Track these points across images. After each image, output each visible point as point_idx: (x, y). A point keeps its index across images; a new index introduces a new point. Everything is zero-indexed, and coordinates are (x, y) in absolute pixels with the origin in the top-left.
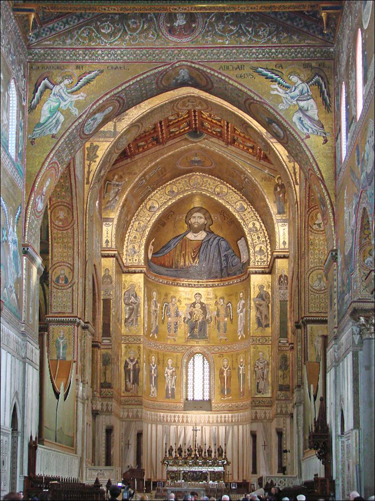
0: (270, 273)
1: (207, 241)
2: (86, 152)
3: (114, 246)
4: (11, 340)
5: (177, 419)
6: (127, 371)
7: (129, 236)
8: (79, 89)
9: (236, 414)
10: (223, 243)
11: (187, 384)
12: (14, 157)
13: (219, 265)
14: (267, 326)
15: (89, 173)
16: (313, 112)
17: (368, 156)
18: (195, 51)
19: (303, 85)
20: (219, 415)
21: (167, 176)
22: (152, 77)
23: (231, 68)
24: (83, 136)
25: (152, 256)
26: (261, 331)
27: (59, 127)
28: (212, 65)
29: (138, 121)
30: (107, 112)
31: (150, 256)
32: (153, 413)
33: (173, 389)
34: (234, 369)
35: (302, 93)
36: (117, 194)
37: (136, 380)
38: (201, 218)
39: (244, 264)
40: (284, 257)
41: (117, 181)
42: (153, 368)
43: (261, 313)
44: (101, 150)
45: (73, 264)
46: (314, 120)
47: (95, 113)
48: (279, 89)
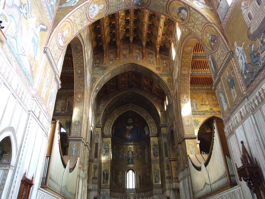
0: (157, 137)
1: (132, 129)
3: (101, 124)
5: (123, 196)
6: (104, 175)
7: (106, 124)
9: (147, 193)
11: (126, 182)
14: (157, 156)
15: (92, 86)
25: (114, 133)
26: (155, 158)
27: (76, 3)
31: (113, 133)
33: (121, 184)
36: (102, 106)
37: (107, 179)
38: (131, 120)
40: (164, 127)
41: (103, 102)
43: (155, 151)
45: (83, 116)
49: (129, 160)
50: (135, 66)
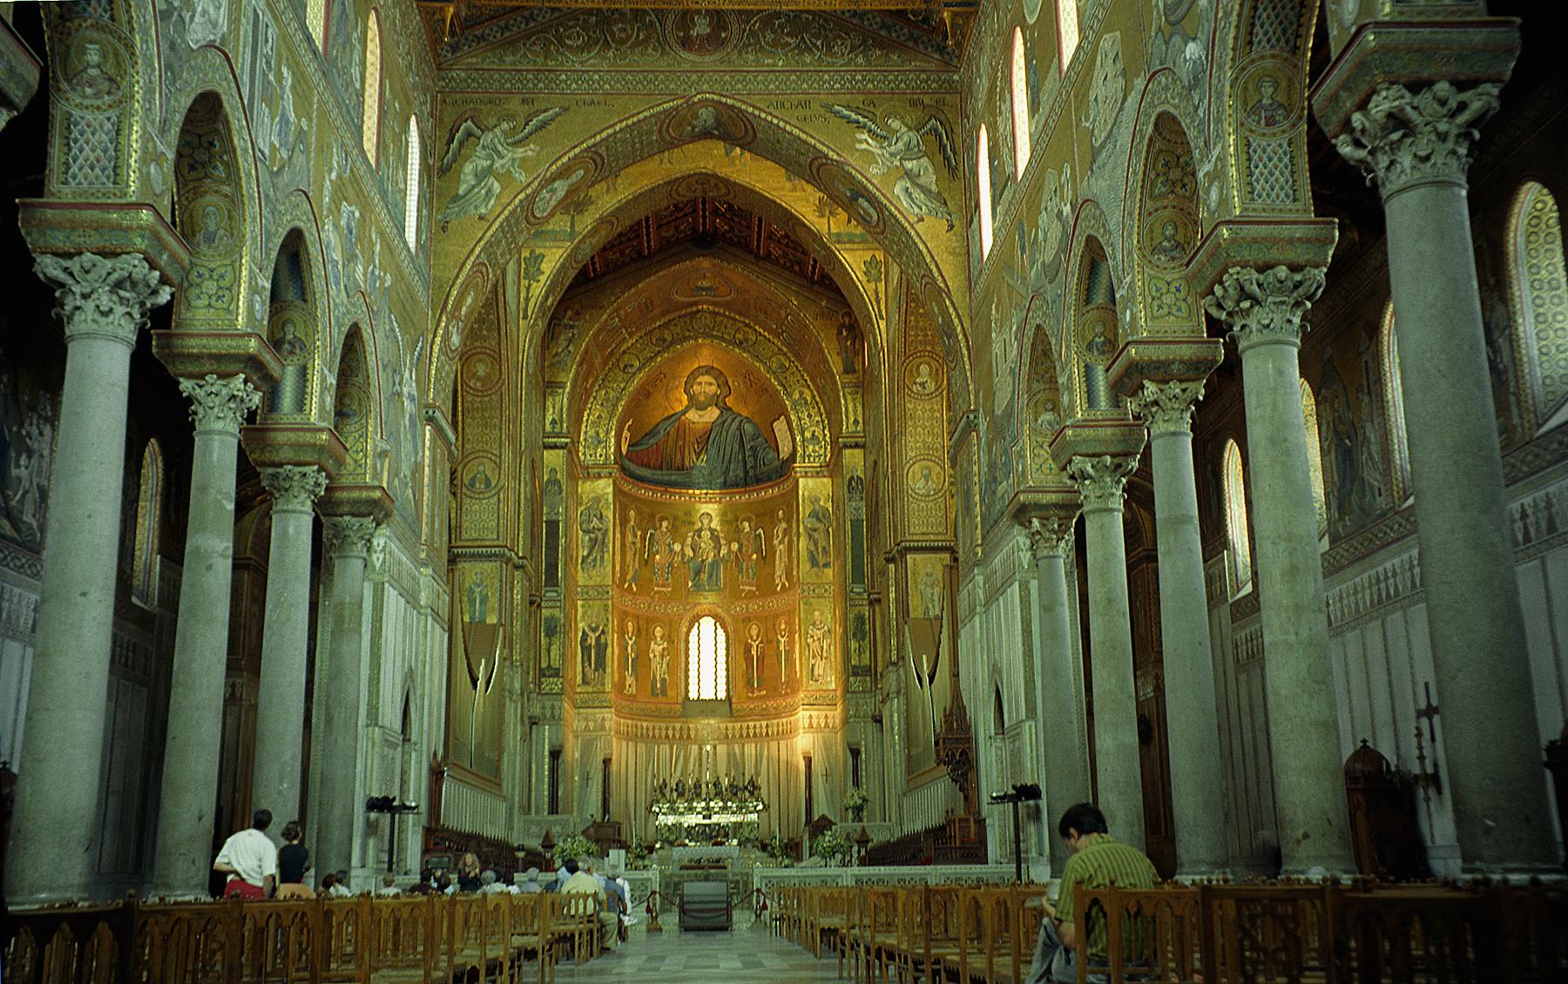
1: (721, 423)
2: (523, 265)
3: (565, 430)
4: (404, 573)
5: (670, 732)
8: (526, 137)
9: (775, 721)
10: (747, 426)
11: (687, 670)
12: (413, 250)
13: (741, 464)
14: (826, 565)
15: (527, 300)
16: (930, 179)
17: (1046, 233)
18: (727, 78)
19: (911, 134)
20: (745, 725)
21: (655, 312)
22: (653, 120)
23: (787, 105)
24: (532, 219)
28: (754, 100)
29: (612, 214)
30: (574, 178)
31: (624, 449)
32: (630, 722)
33: (664, 680)
34: (769, 642)
35: (908, 146)
36: (570, 341)
37: (601, 664)
38: (711, 384)
39: (785, 462)
40: (857, 446)
41: (571, 319)
42: (630, 643)
43: (816, 544)
44: (550, 261)
46: (931, 192)
47: (554, 180)
48: (870, 141)
49: (698, 573)
50: (720, 185)
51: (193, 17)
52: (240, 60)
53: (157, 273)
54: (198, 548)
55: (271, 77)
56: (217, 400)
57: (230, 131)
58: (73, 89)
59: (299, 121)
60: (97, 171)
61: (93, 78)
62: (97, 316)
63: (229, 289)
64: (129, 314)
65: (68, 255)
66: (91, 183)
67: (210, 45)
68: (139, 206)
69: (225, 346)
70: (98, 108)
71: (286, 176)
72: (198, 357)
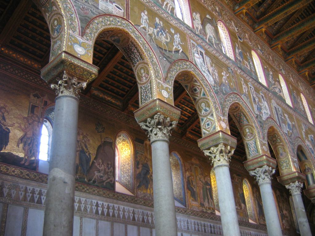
51: (262, 115)
52: (275, 118)
53: (271, 168)
54: (300, 222)
55: (283, 118)
56: (294, 188)
57: (278, 132)
58: (246, 138)
59: (292, 123)
60: (254, 152)
61: (249, 135)
62: (262, 180)
63: (289, 164)
64: (268, 178)
65: (254, 170)
66: (254, 154)
67: (268, 118)
68: (263, 156)
69: (291, 176)
70: (251, 140)
71: (293, 136)
72: (287, 180)
